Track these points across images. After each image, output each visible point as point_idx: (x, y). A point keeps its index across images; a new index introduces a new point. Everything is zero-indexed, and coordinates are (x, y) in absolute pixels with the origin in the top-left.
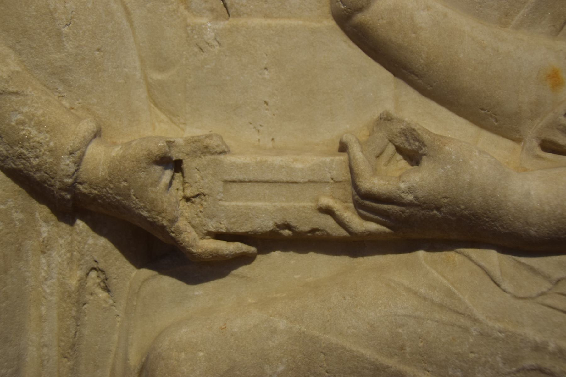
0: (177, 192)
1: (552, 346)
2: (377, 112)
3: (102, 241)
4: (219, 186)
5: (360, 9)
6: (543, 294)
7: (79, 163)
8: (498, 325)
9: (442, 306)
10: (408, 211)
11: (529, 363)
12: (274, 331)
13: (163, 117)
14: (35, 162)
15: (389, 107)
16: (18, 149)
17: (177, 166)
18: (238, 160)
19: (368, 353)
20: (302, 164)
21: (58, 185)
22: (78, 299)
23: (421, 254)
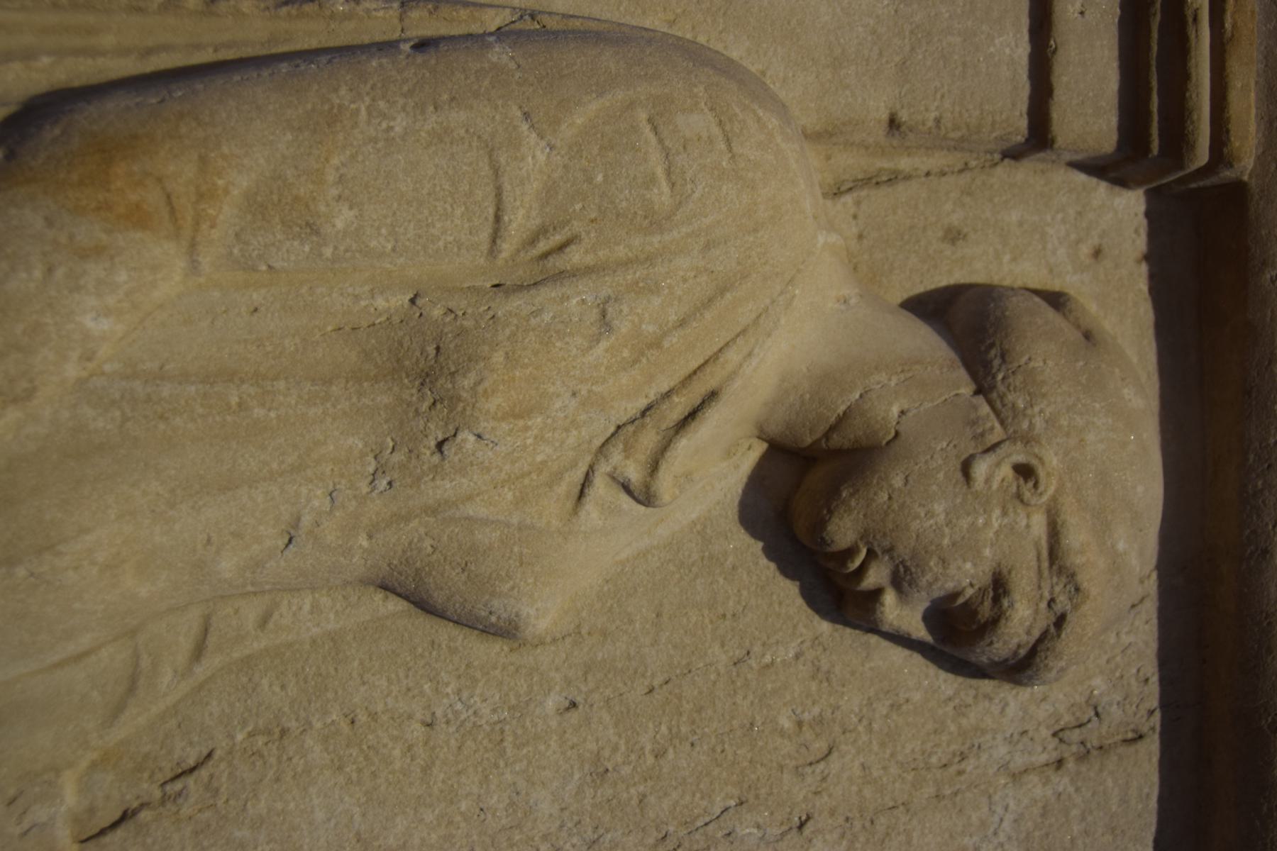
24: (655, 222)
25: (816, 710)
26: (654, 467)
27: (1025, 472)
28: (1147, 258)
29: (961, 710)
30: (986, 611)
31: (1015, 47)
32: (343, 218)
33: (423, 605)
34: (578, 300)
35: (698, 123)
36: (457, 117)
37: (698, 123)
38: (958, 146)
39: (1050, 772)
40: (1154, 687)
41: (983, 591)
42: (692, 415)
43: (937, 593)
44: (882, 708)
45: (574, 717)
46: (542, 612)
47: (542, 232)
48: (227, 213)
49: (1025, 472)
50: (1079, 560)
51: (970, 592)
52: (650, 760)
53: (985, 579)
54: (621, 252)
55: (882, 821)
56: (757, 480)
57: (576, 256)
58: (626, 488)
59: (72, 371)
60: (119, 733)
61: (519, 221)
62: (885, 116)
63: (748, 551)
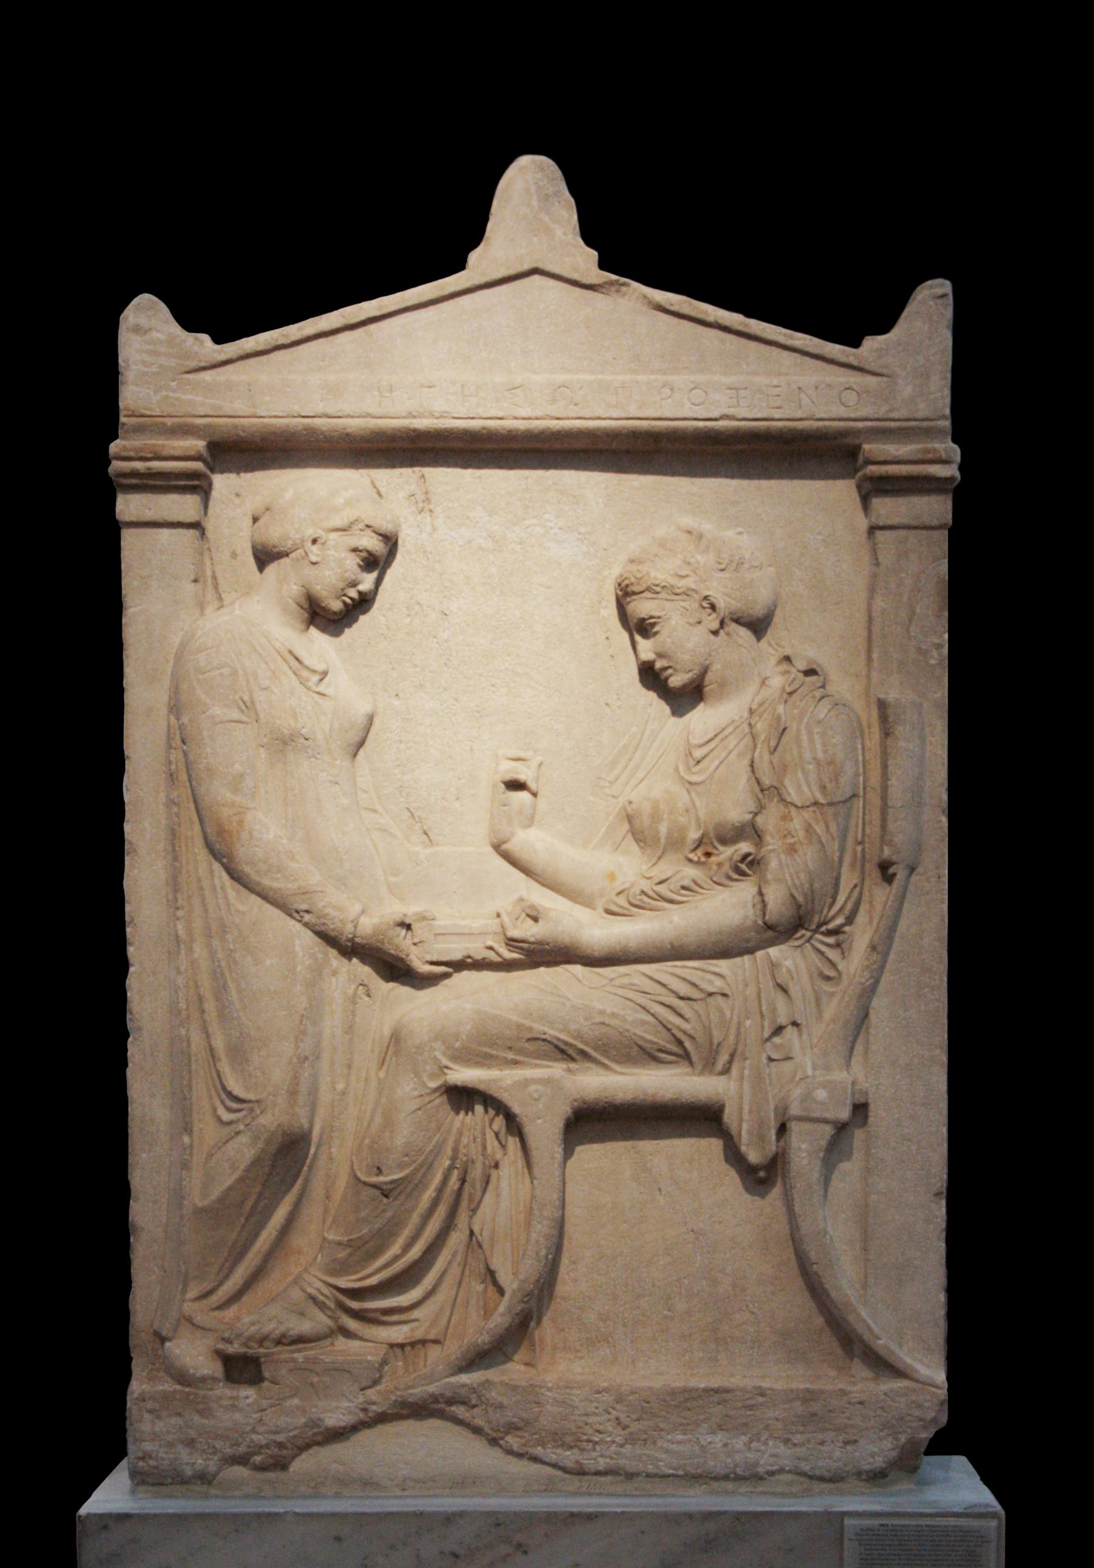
0: (408, 941)
1: (608, 1011)
2: (516, 896)
3: (367, 969)
4: (432, 937)
5: (504, 842)
7: (355, 927)
9: (552, 994)
10: (532, 946)
11: (597, 1020)
14: (332, 927)
15: (523, 893)
16: (323, 920)
17: (408, 927)
18: (443, 922)
19: (514, 1018)
20: (477, 924)
22: (353, 1000)
23: (542, 969)
26: (314, 671)
32: (238, 767)
33: (361, 744)
34: (260, 697)
35: (202, 658)
36: (205, 733)
37: (202, 658)
38: (202, 554)
41: (358, 556)
42: (297, 659)
43: (359, 570)
45: (401, 695)
46: (363, 707)
47: (239, 708)
51: (358, 560)
54: (244, 683)
57: (246, 698)
58: (321, 680)
59: (285, 841)
61: (235, 715)
62: (193, 584)
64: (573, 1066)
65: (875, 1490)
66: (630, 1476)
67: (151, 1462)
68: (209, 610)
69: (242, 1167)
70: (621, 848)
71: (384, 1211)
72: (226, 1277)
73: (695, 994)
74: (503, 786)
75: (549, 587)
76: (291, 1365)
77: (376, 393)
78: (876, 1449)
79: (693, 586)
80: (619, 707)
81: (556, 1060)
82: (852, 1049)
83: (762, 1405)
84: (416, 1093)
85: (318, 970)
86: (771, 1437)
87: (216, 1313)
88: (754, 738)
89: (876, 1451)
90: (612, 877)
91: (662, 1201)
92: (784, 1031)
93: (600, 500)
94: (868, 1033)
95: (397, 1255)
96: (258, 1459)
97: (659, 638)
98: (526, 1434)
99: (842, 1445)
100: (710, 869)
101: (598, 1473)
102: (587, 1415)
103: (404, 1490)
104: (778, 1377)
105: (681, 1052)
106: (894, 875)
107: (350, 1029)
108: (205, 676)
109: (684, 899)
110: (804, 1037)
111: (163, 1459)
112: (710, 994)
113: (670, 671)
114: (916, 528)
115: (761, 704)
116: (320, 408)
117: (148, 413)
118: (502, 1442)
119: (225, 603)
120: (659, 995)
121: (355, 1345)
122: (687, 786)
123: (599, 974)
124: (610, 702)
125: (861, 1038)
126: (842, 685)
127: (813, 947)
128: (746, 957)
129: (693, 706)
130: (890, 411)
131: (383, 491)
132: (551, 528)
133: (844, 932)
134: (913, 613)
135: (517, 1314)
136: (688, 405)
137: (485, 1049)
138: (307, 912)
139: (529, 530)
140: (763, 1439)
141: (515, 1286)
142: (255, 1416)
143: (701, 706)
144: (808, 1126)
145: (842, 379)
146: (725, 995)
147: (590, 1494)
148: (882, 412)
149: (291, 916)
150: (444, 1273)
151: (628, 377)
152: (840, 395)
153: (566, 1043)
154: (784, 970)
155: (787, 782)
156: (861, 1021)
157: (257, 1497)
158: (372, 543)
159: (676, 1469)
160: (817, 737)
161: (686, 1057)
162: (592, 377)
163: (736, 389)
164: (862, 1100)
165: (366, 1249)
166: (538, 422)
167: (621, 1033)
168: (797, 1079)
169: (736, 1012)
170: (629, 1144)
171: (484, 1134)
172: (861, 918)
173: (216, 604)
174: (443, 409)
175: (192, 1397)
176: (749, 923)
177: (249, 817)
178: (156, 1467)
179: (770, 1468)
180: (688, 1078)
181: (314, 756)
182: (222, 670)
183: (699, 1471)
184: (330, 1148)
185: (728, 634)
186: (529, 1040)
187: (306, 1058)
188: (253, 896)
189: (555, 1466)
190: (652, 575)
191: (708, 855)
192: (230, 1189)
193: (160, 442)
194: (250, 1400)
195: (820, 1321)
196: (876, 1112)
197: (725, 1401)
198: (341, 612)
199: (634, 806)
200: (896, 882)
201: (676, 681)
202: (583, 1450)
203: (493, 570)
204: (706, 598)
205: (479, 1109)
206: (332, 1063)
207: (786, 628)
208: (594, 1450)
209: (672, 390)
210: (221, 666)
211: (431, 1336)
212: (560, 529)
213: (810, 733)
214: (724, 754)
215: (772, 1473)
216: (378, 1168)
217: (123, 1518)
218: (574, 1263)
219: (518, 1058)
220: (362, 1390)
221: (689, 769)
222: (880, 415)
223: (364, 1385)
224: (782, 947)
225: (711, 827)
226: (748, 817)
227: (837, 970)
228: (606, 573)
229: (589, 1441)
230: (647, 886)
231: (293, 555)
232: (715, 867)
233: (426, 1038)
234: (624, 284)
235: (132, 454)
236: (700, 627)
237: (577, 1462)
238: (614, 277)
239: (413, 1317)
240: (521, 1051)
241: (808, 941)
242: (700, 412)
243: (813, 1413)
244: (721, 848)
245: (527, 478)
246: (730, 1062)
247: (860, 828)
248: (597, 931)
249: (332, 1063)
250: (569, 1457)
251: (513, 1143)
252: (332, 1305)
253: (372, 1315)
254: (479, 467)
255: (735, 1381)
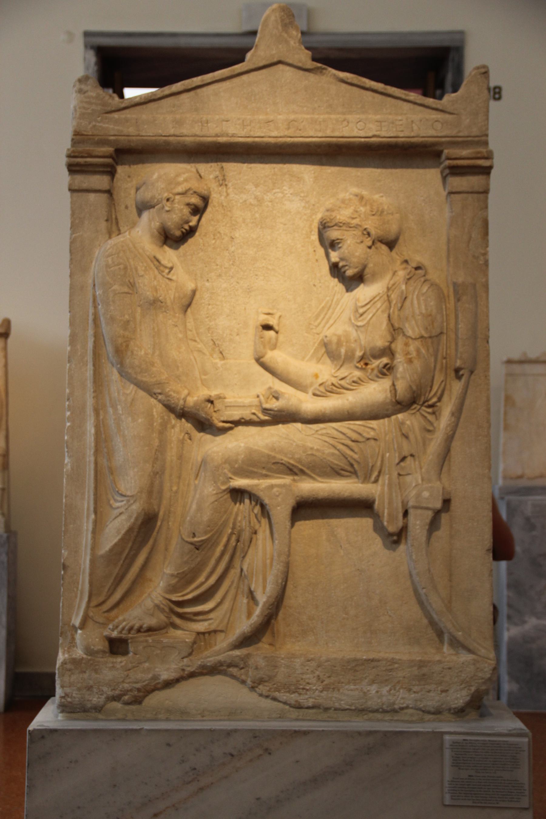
1: (315, 448)
2: (267, 386)
4: (224, 408)
5: (262, 357)
6: (313, 434)
7: (185, 402)
8: (301, 443)
10: (276, 413)
11: (309, 453)
12: (240, 447)
13: (206, 389)
14: (173, 402)
15: (271, 384)
16: (168, 398)
17: (212, 402)
19: (266, 451)
20: (247, 401)
21: (179, 408)
22: (182, 442)
23: (280, 425)
24: (126, 268)
25: (212, 236)
26: (166, 267)
27: (168, 200)
28: (130, 165)
29: (214, 206)
30: (193, 207)
31: (92, 197)
33: (189, 305)
39: (228, 187)
40: (213, 164)
42: (158, 261)
43: (190, 215)
44: (212, 223)
45: (210, 280)
46: (191, 286)
47: (128, 286)
48: (127, 333)
49: (168, 200)
50: (184, 189)
51: (190, 210)
52: (218, 267)
53: (187, 207)
55: (233, 222)
56: (171, 247)
57: (131, 281)
58: (170, 272)
60: (208, 353)
61: (126, 289)
63: (183, 248)
64: (296, 478)
65: (458, 719)
66: (326, 709)
67: (69, 700)
68: (114, 235)
69: (123, 532)
70: (321, 361)
71: (197, 557)
72: (112, 594)
73: (361, 439)
74: (261, 328)
75: (285, 225)
76: (145, 644)
77: (200, 124)
78: (458, 696)
79: (359, 223)
80: (320, 287)
81: (287, 474)
82: (441, 469)
83: (396, 669)
84: (215, 492)
85: (164, 425)
86: (401, 688)
87: (106, 614)
88: (390, 302)
89: (459, 697)
90: (316, 376)
91: (342, 553)
92: (406, 459)
93: (311, 180)
94: (450, 461)
95: (203, 581)
96: (126, 697)
97: (342, 250)
98: (270, 685)
99: (439, 692)
100: (367, 372)
101: (308, 708)
102: (302, 674)
103: (203, 716)
104: (404, 653)
105: (352, 470)
106: (463, 375)
107: (180, 457)
108: (112, 269)
109: (354, 388)
110: (417, 463)
111: (75, 698)
112: (368, 439)
113: (347, 268)
114: (472, 193)
115: (393, 285)
116: (172, 132)
117: (85, 133)
118: (257, 689)
119: (122, 232)
120: (342, 439)
121: (179, 633)
122: (356, 327)
123: (311, 428)
124: (316, 284)
125: (446, 463)
126: (433, 275)
127: (421, 413)
128: (386, 420)
129: (357, 286)
130: (459, 132)
131: (202, 174)
132: (287, 194)
133: (437, 406)
134: (470, 238)
135: (266, 616)
136: (356, 130)
137: (251, 469)
138: (160, 394)
139: (276, 195)
140: (397, 688)
141: (264, 599)
142: (125, 673)
143: (362, 286)
144: (419, 511)
145: (434, 116)
146: (375, 440)
147: (303, 720)
148: (454, 132)
149: (152, 396)
150: (227, 592)
151: (326, 116)
152: (432, 125)
153: (293, 465)
154: (406, 426)
155: (407, 325)
156: (445, 455)
157: (124, 720)
158: (195, 200)
159: (350, 706)
160: (422, 302)
161: (354, 473)
162: (309, 116)
163: (380, 122)
164: (447, 497)
165: (185, 579)
166: (280, 139)
167: (321, 460)
168: (414, 485)
169: (381, 448)
170: (325, 521)
171: (250, 515)
172: (445, 398)
173: (117, 233)
174: (233, 132)
175: (91, 662)
176: (388, 401)
177: (132, 343)
178: (70, 702)
179: (401, 706)
180: (356, 485)
181: (165, 312)
182: (120, 266)
183: (363, 707)
184: (168, 522)
185: (376, 248)
186: (274, 463)
187: (158, 473)
188: (132, 386)
189: (285, 703)
190: (338, 217)
191: (366, 364)
192: (116, 544)
193: (91, 149)
194: (123, 664)
195: (425, 621)
196: (454, 504)
197: (377, 667)
198: (180, 237)
199: (328, 339)
200: (464, 379)
201: (350, 272)
202: (300, 694)
203: (257, 215)
204: (365, 229)
205: (247, 501)
206: (171, 476)
207: (406, 246)
208: (306, 694)
209: (348, 122)
210: (119, 264)
211: (219, 628)
212: (291, 194)
213: (418, 299)
214: (374, 311)
215: (402, 709)
216: (194, 534)
217: (53, 731)
218: (296, 587)
219: (267, 473)
220: (183, 658)
221: (356, 319)
222: (453, 135)
223: (183, 656)
224: (406, 414)
225: (368, 349)
226: (387, 344)
227: (433, 426)
228: (314, 217)
229: (303, 689)
230: (334, 381)
231: (156, 207)
232: (370, 371)
233: (220, 462)
234: (324, 69)
235: (77, 154)
236: (362, 244)
237: (296, 701)
238: (319, 65)
239: (210, 617)
240: (269, 470)
241: (418, 411)
242: (362, 134)
243: (423, 674)
244: (373, 361)
245: (274, 168)
246: (378, 476)
247: (445, 350)
248: (310, 404)
249: (171, 476)
250: (293, 698)
251: (264, 522)
252: (167, 610)
253: (188, 616)
254: (251, 163)
255: (382, 655)
